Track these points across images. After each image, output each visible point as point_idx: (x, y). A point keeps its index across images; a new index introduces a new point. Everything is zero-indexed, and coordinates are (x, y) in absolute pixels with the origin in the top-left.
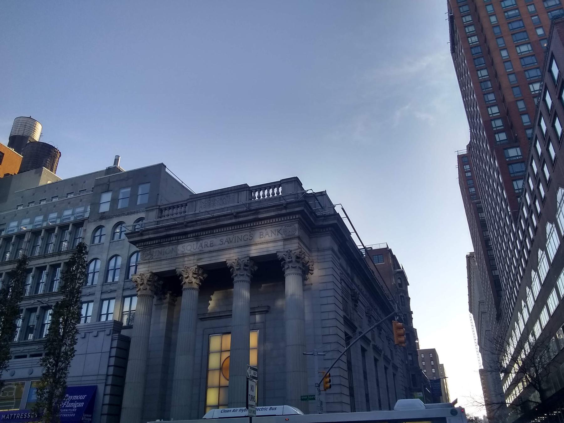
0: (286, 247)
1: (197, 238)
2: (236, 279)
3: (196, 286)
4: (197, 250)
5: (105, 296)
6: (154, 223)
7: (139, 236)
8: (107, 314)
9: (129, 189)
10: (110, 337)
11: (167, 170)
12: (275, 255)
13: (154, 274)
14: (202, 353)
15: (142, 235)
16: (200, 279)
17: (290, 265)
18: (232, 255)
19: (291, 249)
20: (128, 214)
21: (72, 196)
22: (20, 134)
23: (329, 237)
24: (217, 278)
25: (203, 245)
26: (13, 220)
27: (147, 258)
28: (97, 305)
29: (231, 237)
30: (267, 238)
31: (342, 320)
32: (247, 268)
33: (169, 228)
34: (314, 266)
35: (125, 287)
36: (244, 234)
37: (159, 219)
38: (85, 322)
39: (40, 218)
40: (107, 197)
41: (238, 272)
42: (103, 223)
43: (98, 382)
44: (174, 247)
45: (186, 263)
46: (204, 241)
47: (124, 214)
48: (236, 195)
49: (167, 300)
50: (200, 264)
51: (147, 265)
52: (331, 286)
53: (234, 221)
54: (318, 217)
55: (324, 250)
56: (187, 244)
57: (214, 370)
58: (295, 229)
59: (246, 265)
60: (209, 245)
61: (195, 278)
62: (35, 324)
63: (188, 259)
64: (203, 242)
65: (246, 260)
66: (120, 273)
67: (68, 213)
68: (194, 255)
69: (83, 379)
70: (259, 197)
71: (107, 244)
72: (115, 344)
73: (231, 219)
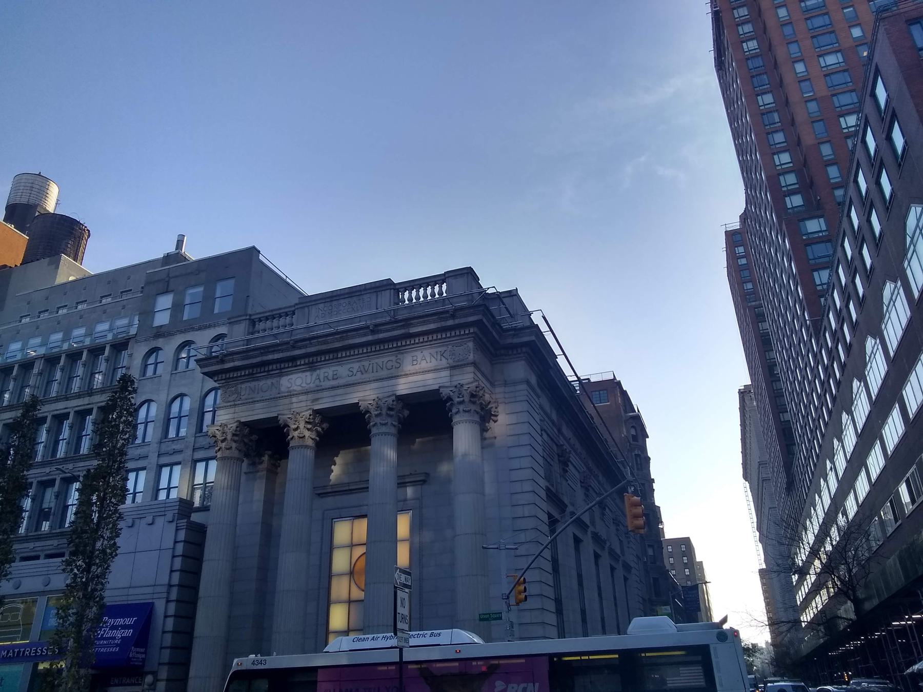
0: (455, 378)
2: (374, 431)
3: (310, 443)
4: (312, 385)
5: (165, 460)
6: (242, 343)
7: (218, 363)
8: (169, 489)
9: (200, 289)
10: (174, 525)
11: (261, 257)
12: (437, 391)
13: (243, 425)
14: (321, 549)
15: (222, 361)
16: (317, 431)
17: (461, 407)
18: (368, 393)
19: (461, 382)
20: (200, 329)
21: (109, 300)
23: (523, 362)
24: (343, 429)
25: (322, 377)
26: (14, 340)
27: (231, 398)
28: (153, 474)
29: (366, 363)
30: (424, 365)
31: (543, 494)
32: (392, 413)
33: (266, 350)
34: (499, 409)
35: (197, 445)
36: (386, 359)
37: (250, 337)
38: (133, 501)
39: (58, 336)
40: (165, 302)
41: (378, 420)
42: (159, 343)
43: (156, 596)
44: (274, 380)
45: (295, 405)
46: (323, 371)
47: (193, 329)
48: (374, 297)
49: (265, 465)
50: (316, 407)
51: (232, 410)
52: (525, 440)
53: (370, 338)
55: (515, 383)
56: (294, 376)
57: (340, 575)
58: (468, 350)
59: (390, 409)
60: (330, 377)
61: (308, 429)
62: (52, 505)
63: (297, 397)
64: (321, 372)
65: (390, 400)
66: (189, 424)
67: (102, 327)
68: (307, 393)
69: (131, 591)
70: (410, 299)
71: (166, 377)
72: (182, 535)
73: (365, 335)
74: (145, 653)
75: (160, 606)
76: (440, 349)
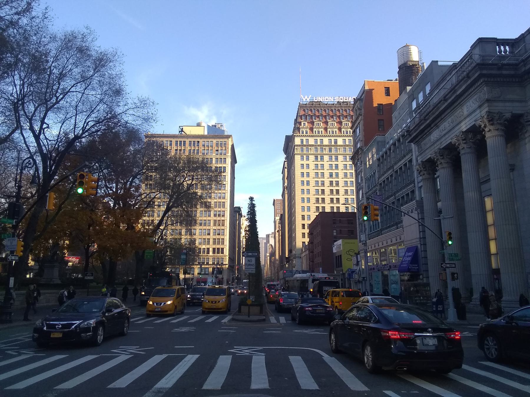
11: (439, 63)
22: (402, 62)
29: (453, 117)
36: (458, 112)
54: (517, 65)
56: (434, 133)
64: (442, 127)
73: (444, 103)
74: (418, 266)
75: (419, 246)
76: (475, 97)
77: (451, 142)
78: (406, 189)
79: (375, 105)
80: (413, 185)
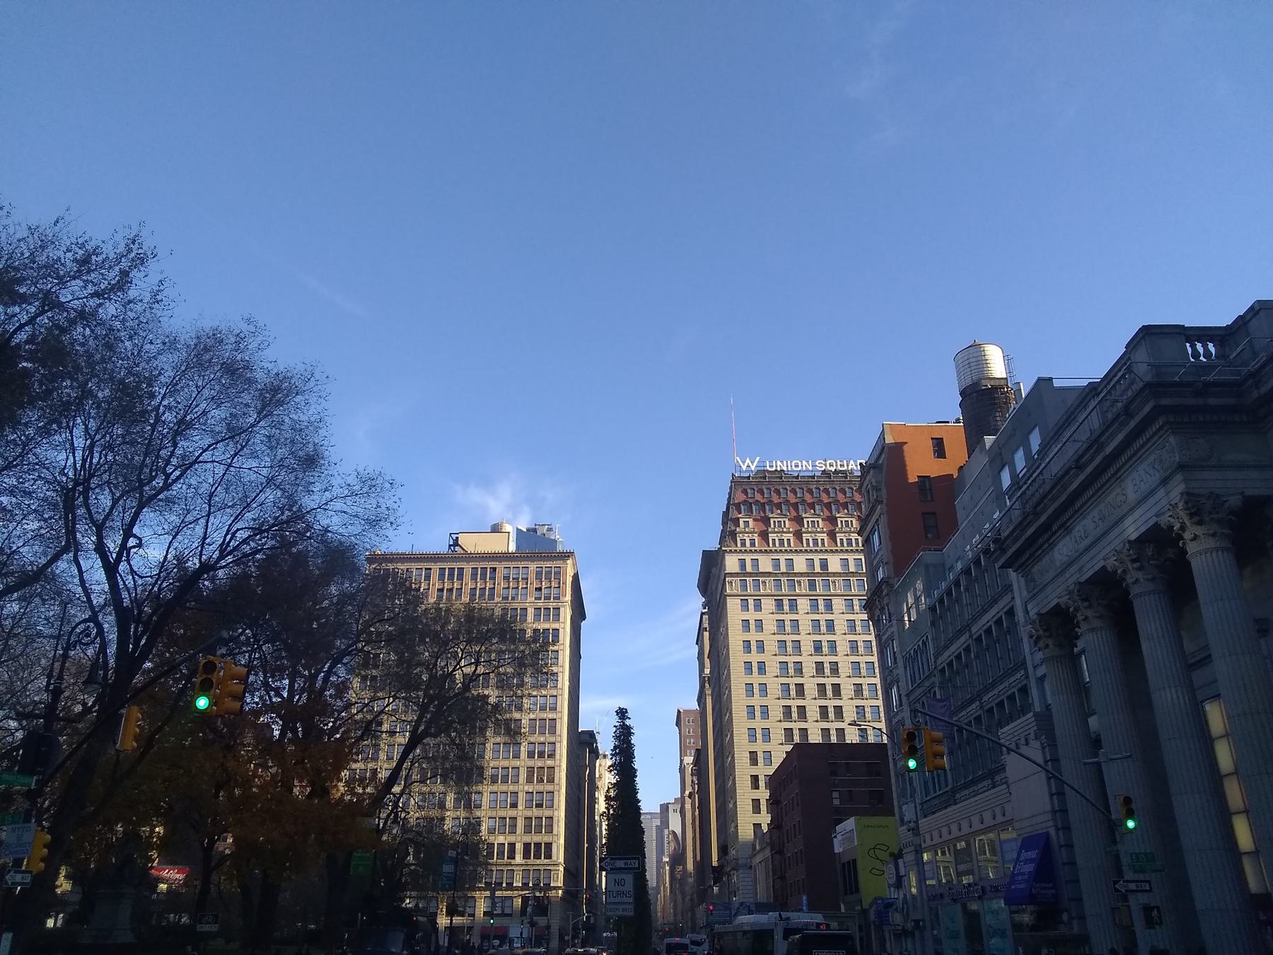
1: (1066, 529)
11: (1056, 383)
36: (1114, 493)
46: (1077, 529)
56: (1060, 545)
75: (1052, 832)
76: (1152, 458)
77: (1104, 568)
78: (1006, 684)
79: (912, 478)
80: (1022, 672)
